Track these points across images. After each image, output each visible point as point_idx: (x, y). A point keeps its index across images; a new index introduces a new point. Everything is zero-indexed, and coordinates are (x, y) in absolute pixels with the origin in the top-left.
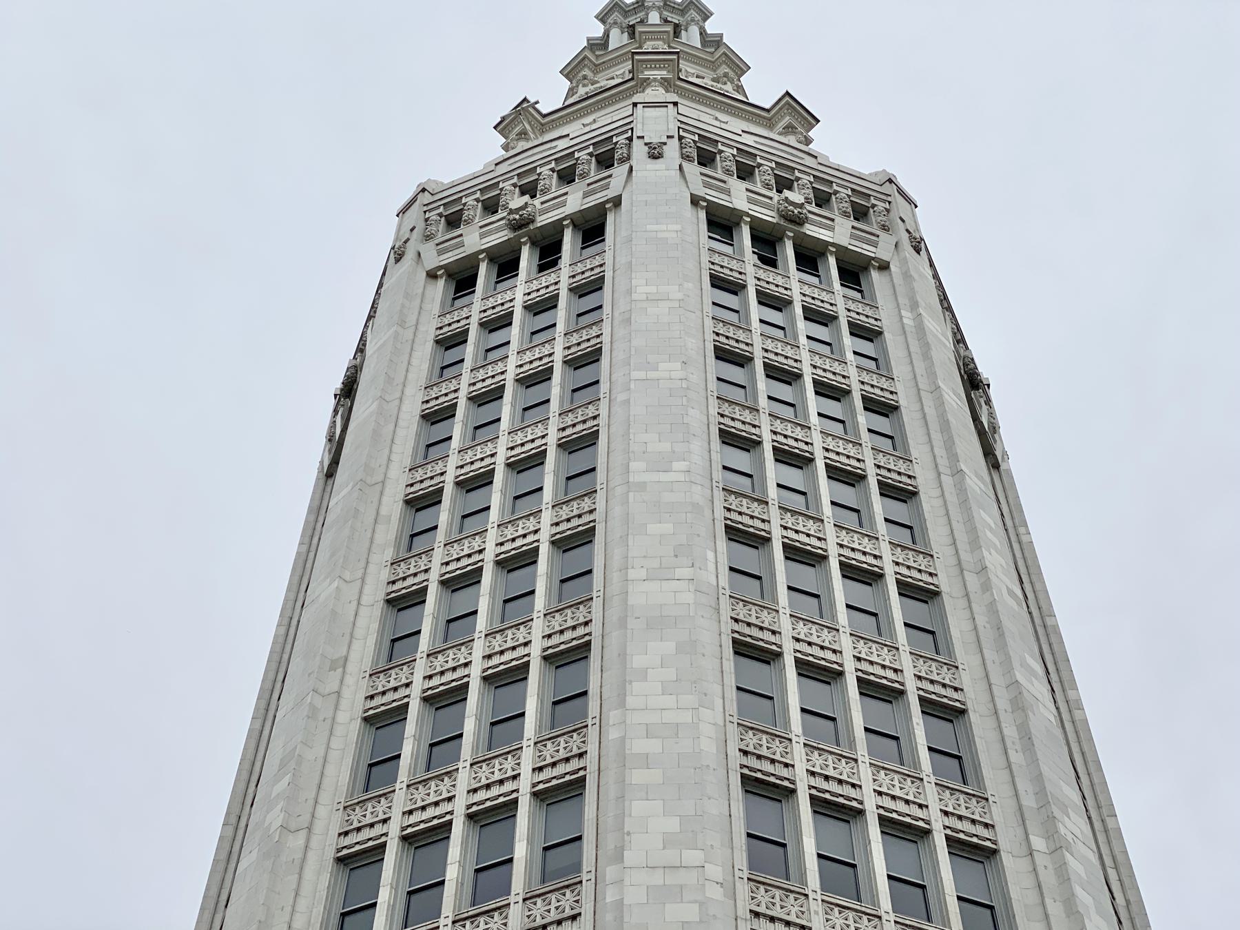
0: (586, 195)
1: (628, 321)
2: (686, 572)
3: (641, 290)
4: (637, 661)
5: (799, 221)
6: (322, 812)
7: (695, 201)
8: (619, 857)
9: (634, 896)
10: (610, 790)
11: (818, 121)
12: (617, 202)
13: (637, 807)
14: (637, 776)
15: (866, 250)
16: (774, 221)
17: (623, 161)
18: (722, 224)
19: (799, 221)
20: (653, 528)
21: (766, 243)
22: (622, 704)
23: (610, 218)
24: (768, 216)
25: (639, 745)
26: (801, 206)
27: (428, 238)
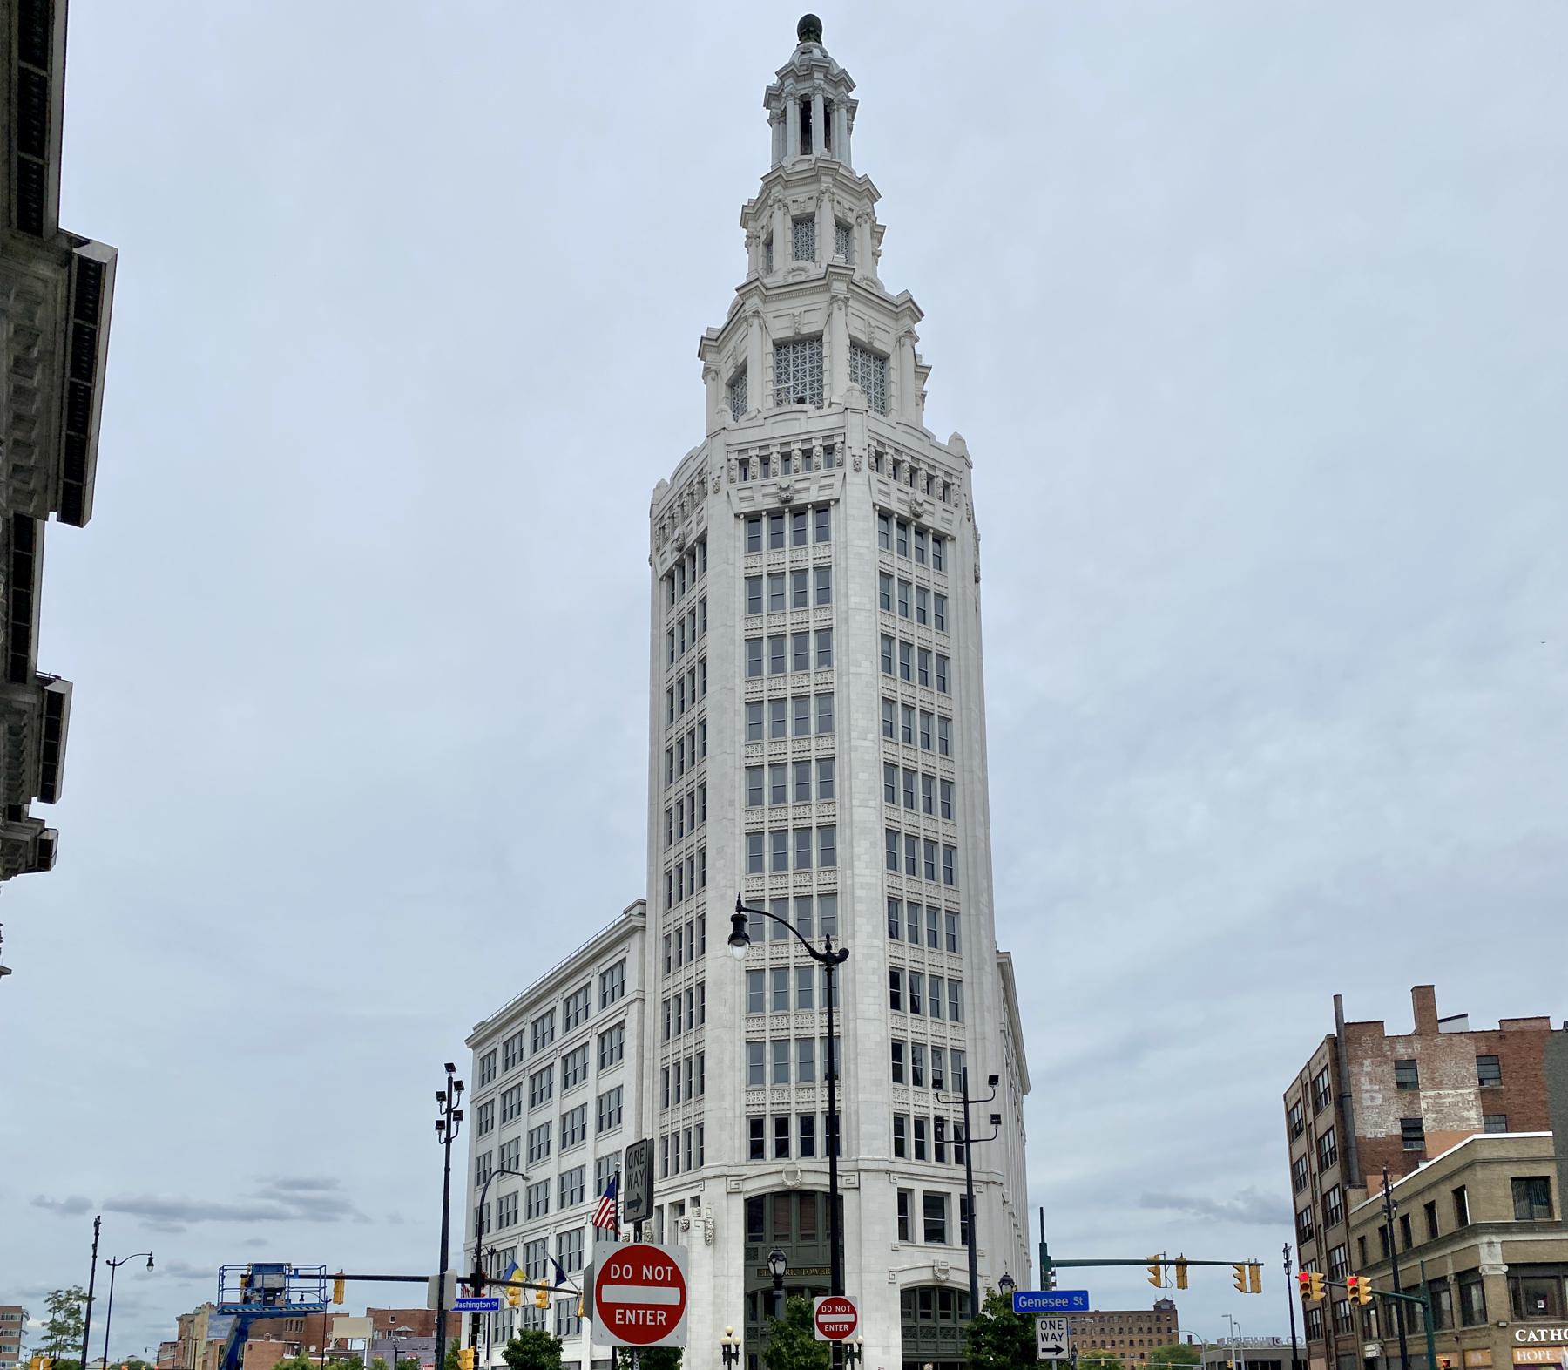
0: (822, 488)
1: (847, 620)
2: (872, 803)
3: (853, 600)
4: (857, 850)
5: (918, 516)
12: (837, 501)
13: (859, 920)
14: (859, 907)
15: (943, 528)
17: (840, 465)
18: (885, 515)
19: (918, 516)
20: (863, 776)
21: (903, 524)
22: (852, 867)
23: (832, 510)
24: (904, 511)
25: (859, 893)
27: (732, 481)
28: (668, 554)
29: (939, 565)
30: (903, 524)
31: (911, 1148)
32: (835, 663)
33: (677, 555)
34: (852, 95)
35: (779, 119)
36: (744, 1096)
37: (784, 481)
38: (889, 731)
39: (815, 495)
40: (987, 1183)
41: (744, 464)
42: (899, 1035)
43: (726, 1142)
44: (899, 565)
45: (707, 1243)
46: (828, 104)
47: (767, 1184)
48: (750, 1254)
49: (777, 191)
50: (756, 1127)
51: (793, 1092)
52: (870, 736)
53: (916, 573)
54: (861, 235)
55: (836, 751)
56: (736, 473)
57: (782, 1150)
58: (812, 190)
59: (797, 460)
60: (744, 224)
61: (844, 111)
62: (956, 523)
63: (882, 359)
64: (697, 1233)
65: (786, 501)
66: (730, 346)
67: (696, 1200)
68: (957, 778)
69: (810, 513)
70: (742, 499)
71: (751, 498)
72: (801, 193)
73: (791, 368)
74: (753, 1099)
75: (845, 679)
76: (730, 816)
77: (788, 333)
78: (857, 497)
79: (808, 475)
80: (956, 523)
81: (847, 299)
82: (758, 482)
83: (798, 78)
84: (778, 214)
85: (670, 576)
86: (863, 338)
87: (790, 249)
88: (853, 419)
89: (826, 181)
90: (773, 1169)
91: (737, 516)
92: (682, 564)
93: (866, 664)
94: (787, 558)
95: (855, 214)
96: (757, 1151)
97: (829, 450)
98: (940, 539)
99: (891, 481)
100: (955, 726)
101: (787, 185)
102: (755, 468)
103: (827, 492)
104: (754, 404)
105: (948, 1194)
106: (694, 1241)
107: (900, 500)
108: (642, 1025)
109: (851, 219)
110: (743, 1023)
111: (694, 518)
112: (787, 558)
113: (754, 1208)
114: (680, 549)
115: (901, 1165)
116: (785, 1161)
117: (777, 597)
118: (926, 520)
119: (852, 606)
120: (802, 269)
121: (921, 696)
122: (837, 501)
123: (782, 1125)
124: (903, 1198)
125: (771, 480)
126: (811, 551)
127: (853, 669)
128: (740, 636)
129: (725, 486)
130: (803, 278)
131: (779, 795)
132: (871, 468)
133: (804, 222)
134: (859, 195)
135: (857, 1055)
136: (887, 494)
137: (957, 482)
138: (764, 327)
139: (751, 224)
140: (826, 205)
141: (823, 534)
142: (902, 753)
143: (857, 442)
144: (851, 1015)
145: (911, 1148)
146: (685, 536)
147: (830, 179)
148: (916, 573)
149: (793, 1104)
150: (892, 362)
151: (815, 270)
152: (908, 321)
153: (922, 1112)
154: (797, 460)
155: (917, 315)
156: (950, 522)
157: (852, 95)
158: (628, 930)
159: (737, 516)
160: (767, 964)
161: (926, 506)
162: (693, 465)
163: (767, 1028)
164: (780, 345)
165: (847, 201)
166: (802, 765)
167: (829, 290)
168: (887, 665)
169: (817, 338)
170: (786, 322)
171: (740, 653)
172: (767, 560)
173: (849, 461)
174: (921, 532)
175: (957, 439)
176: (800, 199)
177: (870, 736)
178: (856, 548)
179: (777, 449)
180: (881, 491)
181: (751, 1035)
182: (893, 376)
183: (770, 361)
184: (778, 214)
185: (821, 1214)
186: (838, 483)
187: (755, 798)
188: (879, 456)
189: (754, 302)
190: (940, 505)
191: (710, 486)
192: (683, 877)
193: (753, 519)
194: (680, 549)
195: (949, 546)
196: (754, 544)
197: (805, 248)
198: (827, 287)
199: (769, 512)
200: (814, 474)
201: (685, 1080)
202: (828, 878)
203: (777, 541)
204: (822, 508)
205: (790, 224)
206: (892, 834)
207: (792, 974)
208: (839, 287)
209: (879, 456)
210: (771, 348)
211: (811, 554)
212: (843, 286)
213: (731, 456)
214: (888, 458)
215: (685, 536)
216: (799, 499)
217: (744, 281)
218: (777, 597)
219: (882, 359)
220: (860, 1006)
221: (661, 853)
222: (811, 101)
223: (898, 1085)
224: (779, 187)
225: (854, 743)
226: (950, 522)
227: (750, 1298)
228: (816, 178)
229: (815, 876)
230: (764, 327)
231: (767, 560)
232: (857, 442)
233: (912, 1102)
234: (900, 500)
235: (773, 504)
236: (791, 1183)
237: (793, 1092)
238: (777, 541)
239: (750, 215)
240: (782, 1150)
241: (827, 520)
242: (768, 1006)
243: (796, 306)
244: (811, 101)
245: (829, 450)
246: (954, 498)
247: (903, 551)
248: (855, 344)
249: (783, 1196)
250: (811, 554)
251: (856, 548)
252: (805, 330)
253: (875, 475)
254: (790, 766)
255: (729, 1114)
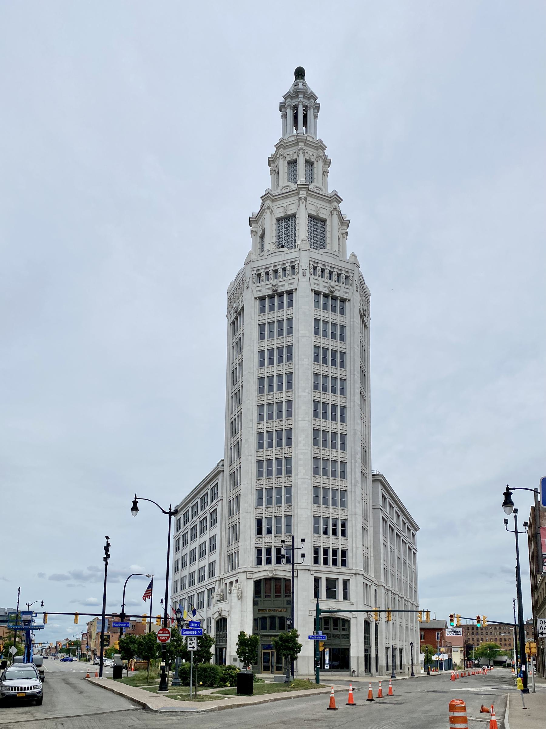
0: (289, 284)
2: (307, 419)
3: (301, 332)
4: (300, 439)
5: (333, 292)
6: (253, 452)
7: (312, 290)
8: (298, 475)
9: (299, 483)
10: (296, 459)
11: (342, 200)
12: (296, 289)
13: (300, 468)
14: (300, 462)
15: (345, 296)
16: (327, 292)
17: (297, 274)
18: (317, 293)
19: (333, 292)
20: (303, 408)
23: (294, 294)
24: (326, 291)
25: (300, 456)
26: (334, 287)
27: (254, 283)
28: (232, 314)
29: (342, 312)
30: (326, 296)
31: (321, 560)
32: (293, 359)
33: (235, 315)
34: (318, 101)
35: (284, 116)
36: (254, 540)
37: (274, 282)
38: (316, 387)
39: (287, 288)
40: (355, 574)
41: (259, 275)
42: (317, 514)
43: (247, 559)
44: (322, 314)
45: (239, 599)
46: (306, 108)
47: (262, 575)
48: (255, 603)
49: (281, 151)
50: (259, 551)
51: (273, 538)
52: (307, 391)
53: (330, 317)
54: (318, 167)
55: (293, 397)
56: (255, 280)
57: (269, 562)
58: (295, 149)
59: (280, 273)
60: (269, 165)
61: (312, 110)
62: (351, 293)
63: (324, 221)
64: (234, 595)
65: (275, 291)
66: (260, 222)
67: (237, 581)
68: (348, 405)
69: (285, 295)
70: (257, 291)
71: (261, 290)
72: (291, 151)
73: (284, 230)
74: (258, 541)
75: (297, 367)
76: (251, 426)
77: (282, 215)
78: (304, 287)
79: (284, 279)
80: (351, 293)
81: (306, 198)
82: (264, 283)
83: (292, 98)
84: (281, 161)
85: (233, 323)
86: (314, 213)
87: (286, 176)
88: (303, 253)
89: (301, 145)
90: (264, 569)
91: (256, 298)
92: (237, 317)
93: (306, 360)
94: (276, 315)
95: (315, 157)
96: (259, 562)
97: (293, 267)
98: (343, 301)
99: (320, 279)
100: (348, 383)
101: (285, 148)
102: (263, 278)
103: (292, 286)
104: (267, 246)
105: (338, 579)
106: (233, 598)
107: (324, 286)
108: (223, 509)
109: (313, 159)
110: (255, 510)
111: (240, 299)
112: (276, 315)
113: (257, 584)
114: (236, 312)
115: (316, 567)
116: (269, 566)
117: (271, 332)
118: (337, 294)
119: (300, 335)
120: (288, 186)
121: (330, 370)
122: (296, 289)
123: (269, 551)
124: (317, 581)
125: (269, 282)
126: (285, 312)
127: (300, 362)
128: (256, 350)
129: (251, 286)
130: (288, 190)
131: (270, 416)
132: (311, 274)
133: (292, 163)
134: (317, 148)
135: (298, 523)
136: (318, 285)
137: (350, 274)
138: (272, 213)
139: (272, 165)
140: (301, 155)
141: (290, 304)
142: (322, 396)
143: (304, 264)
144: (296, 507)
145: (321, 560)
146: (237, 307)
147: (303, 144)
148: (330, 317)
149: (273, 543)
150: (328, 222)
151: (293, 186)
152: (335, 203)
153: (326, 545)
154: (280, 273)
155: (339, 200)
156: (348, 293)
157: (318, 101)
158: (217, 473)
159: (256, 298)
160: (264, 487)
161: (336, 288)
162: (241, 276)
163: (264, 512)
164: (279, 220)
165: (311, 151)
166: (280, 404)
167: (299, 194)
168: (316, 359)
169: (294, 216)
170: (281, 210)
171: (256, 358)
172: (267, 317)
173: (301, 272)
174: (334, 298)
175: (353, 255)
176: (290, 154)
177: (307, 391)
178: (304, 309)
179: (272, 268)
180: (315, 284)
181: (257, 515)
182: (328, 228)
183: (275, 227)
184: (281, 161)
185: (282, 589)
186: (296, 281)
187: (261, 418)
188: (315, 268)
189: (268, 203)
190: (343, 286)
191: (245, 285)
192: (235, 450)
193: (262, 299)
194: (236, 312)
195: (347, 303)
196: (262, 310)
197: (292, 177)
198: (298, 194)
199: (269, 296)
200: (287, 278)
201: (234, 531)
202: (288, 451)
203: (272, 309)
204: (290, 293)
205: (286, 164)
206: (316, 431)
207: (274, 490)
208: (303, 194)
209: (315, 268)
210: (275, 221)
211: (285, 313)
212: (305, 193)
213: (254, 273)
214: (319, 269)
215: (237, 307)
216: (280, 290)
217: (264, 194)
218: (271, 332)
219: (324, 221)
220: (299, 503)
221: (229, 440)
222: (299, 106)
223: (316, 535)
224: (282, 149)
225: (300, 394)
226: (348, 293)
227: (255, 620)
228: (297, 144)
229: (283, 450)
230: (272, 213)
231: (267, 317)
232: (304, 264)
233: (322, 541)
234: (324, 286)
235: (270, 292)
236: (271, 575)
237: (273, 538)
238: (272, 309)
239: (272, 161)
240: (269, 562)
241: (292, 298)
242: (264, 504)
243: (285, 202)
244: (299, 106)
245: (293, 267)
246: (350, 282)
247: (325, 307)
248: (310, 217)
249: (268, 580)
250: (285, 313)
251: (304, 309)
252: (289, 213)
253: (312, 277)
254: (275, 404)
255: (248, 547)
